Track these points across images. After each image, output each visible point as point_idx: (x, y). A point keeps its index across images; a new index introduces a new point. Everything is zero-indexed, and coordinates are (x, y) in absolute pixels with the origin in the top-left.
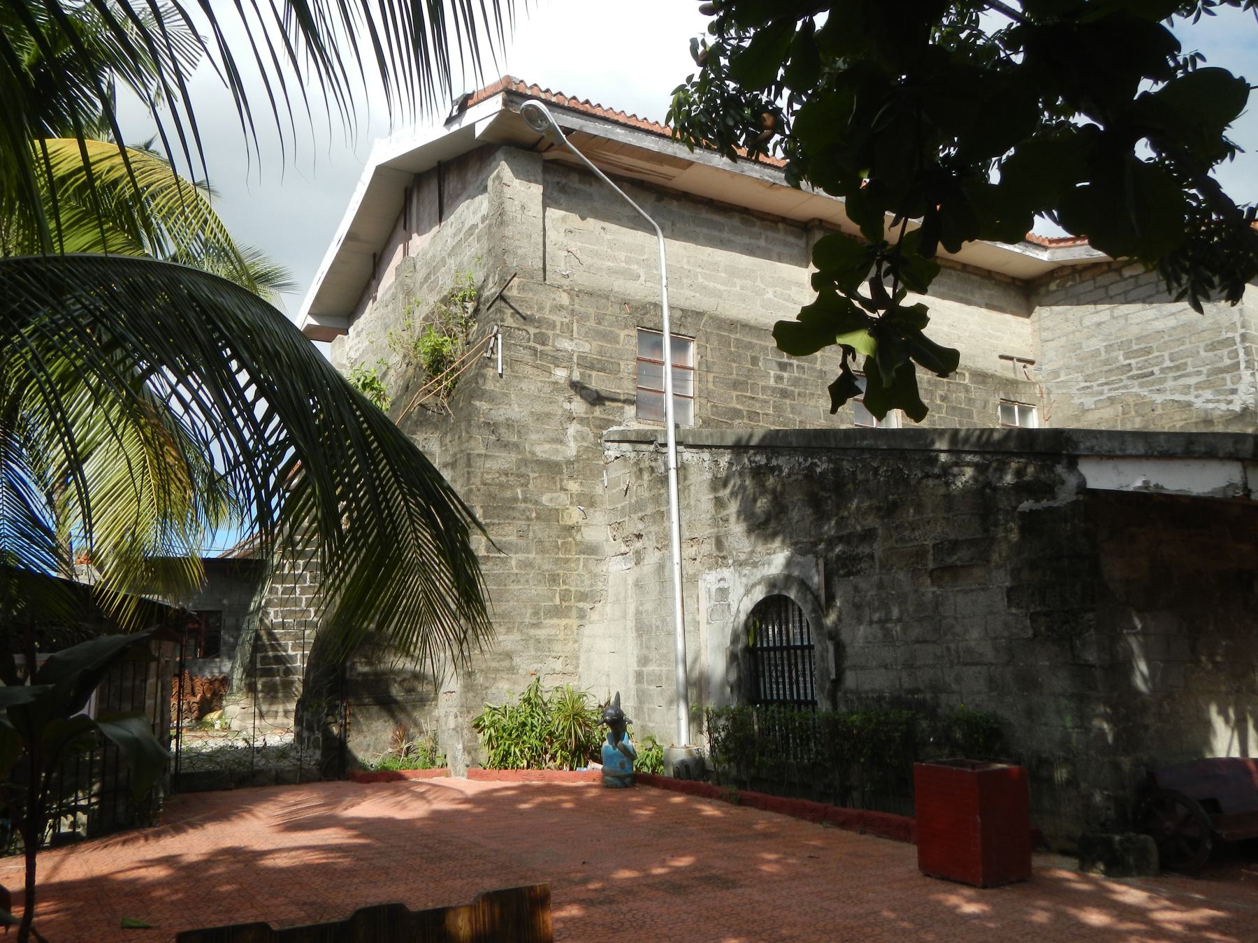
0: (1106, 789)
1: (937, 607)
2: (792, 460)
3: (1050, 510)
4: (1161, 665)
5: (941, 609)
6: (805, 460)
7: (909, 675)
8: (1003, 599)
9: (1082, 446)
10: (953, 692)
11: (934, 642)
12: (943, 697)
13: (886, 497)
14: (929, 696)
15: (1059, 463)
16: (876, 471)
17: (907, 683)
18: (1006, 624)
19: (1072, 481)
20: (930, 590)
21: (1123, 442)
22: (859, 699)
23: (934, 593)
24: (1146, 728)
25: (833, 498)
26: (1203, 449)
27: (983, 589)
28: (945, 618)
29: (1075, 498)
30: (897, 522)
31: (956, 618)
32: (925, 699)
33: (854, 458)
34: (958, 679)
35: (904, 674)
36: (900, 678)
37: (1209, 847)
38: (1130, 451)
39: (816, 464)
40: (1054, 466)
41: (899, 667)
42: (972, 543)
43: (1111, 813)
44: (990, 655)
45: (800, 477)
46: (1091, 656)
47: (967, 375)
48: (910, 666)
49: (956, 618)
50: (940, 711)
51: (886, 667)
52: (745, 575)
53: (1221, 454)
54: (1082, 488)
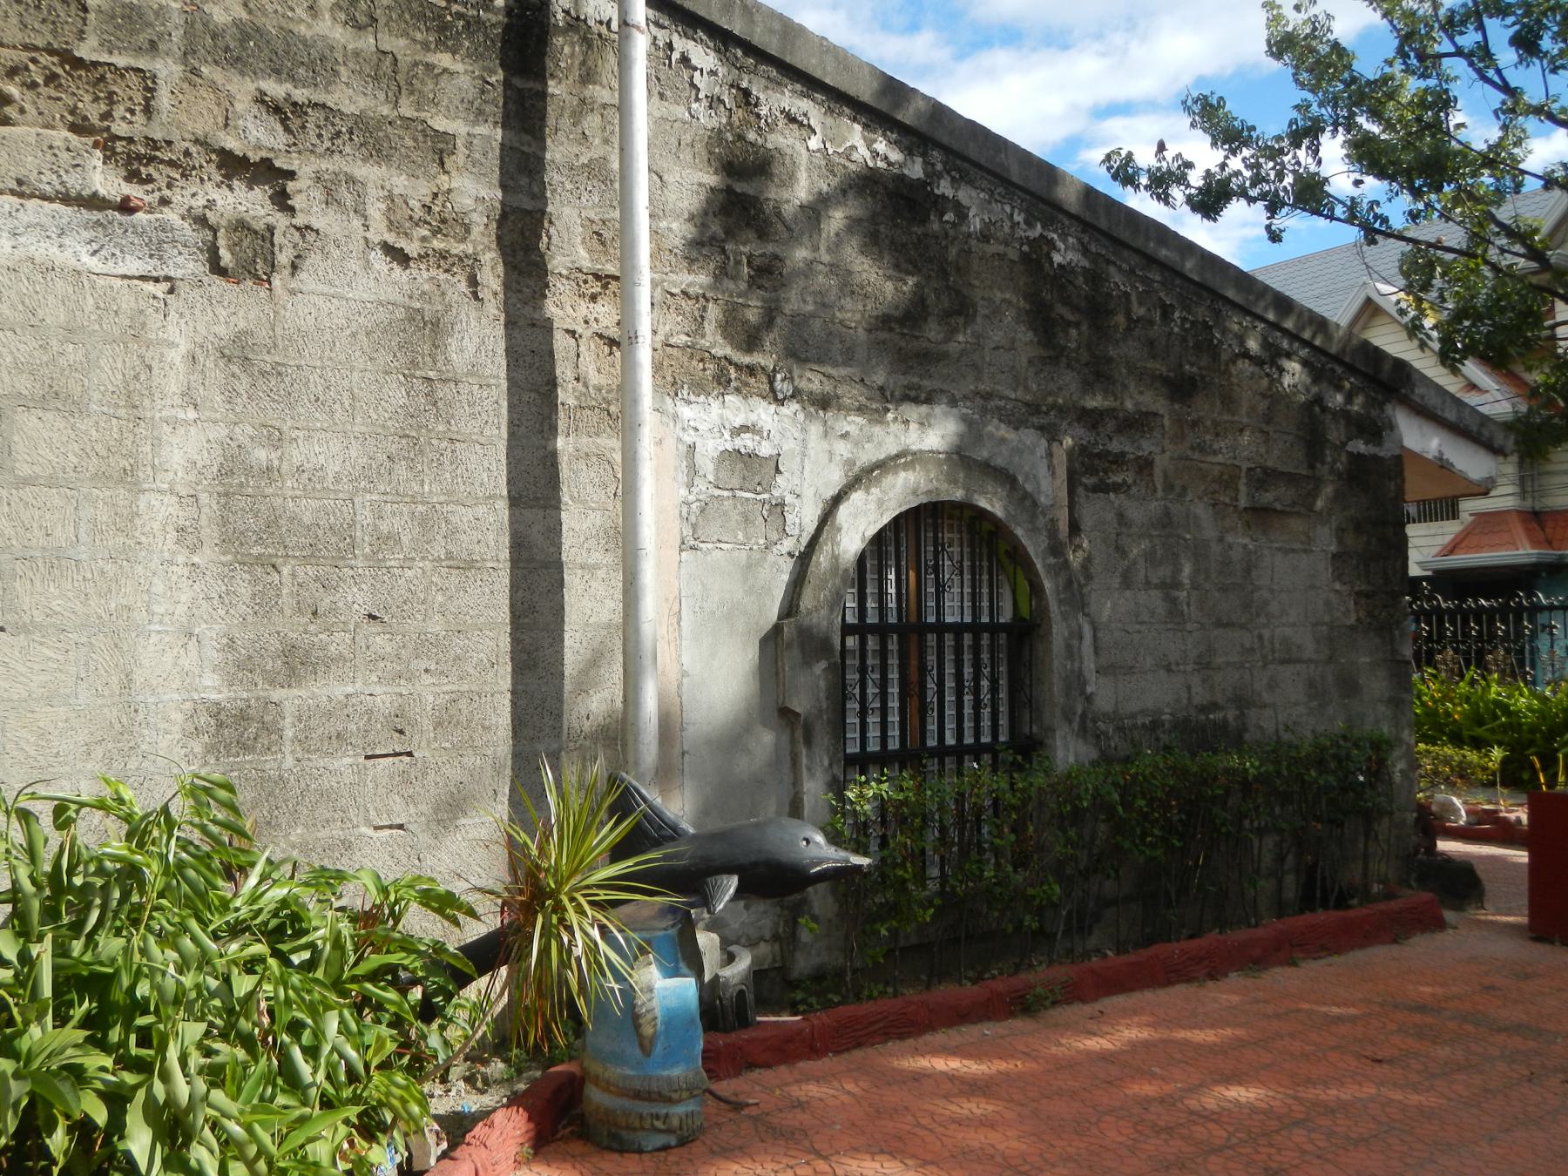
1: (1248, 570)
2: (996, 207)
3: (1375, 459)
5: (1254, 573)
6: (1029, 224)
7: (1204, 681)
8: (1327, 569)
10: (1265, 706)
11: (1242, 627)
12: (1252, 714)
13: (1181, 366)
14: (1231, 714)
16: (1166, 312)
17: (1200, 695)
18: (1328, 603)
20: (1241, 540)
22: (1120, 729)
23: (1245, 546)
25: (1084, 328)
27: (1305, 551)
28: (1259, 588)
30: (1194, 416)
31: (1272, 591)
32: (1225, 720)
33: (1132, 271)
34: (1272, 685)
35: (1195, 681)
36: (1189, 688)
39: (1051, 245)
41: (1189, 668)
42: (1291, 479)
44: (1309, 649)
45: (1013, 255)
48: (1204, 665)
49: (1272, 591)
50: (1247, 736)
51: (1169, 670)
52: (845, 436)
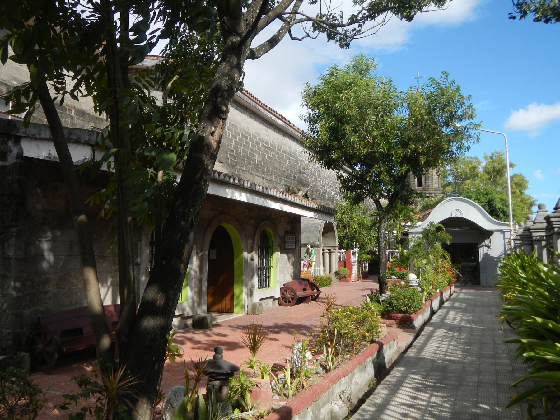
0: (9, 329)
4: (64, 258)
9: (21, 131)
15: (10, 140)
19: (15, 151)
21: (40, 131)
24: (47, 292)
26: (75, 138)
29: (15, 161)
37: (56, 357)
38: (43, 136)
40: (8, 141)
43: (10, 342)
46: (11, 253)
47: (73, 111)
53: (82, 141)
54: (20, 156)
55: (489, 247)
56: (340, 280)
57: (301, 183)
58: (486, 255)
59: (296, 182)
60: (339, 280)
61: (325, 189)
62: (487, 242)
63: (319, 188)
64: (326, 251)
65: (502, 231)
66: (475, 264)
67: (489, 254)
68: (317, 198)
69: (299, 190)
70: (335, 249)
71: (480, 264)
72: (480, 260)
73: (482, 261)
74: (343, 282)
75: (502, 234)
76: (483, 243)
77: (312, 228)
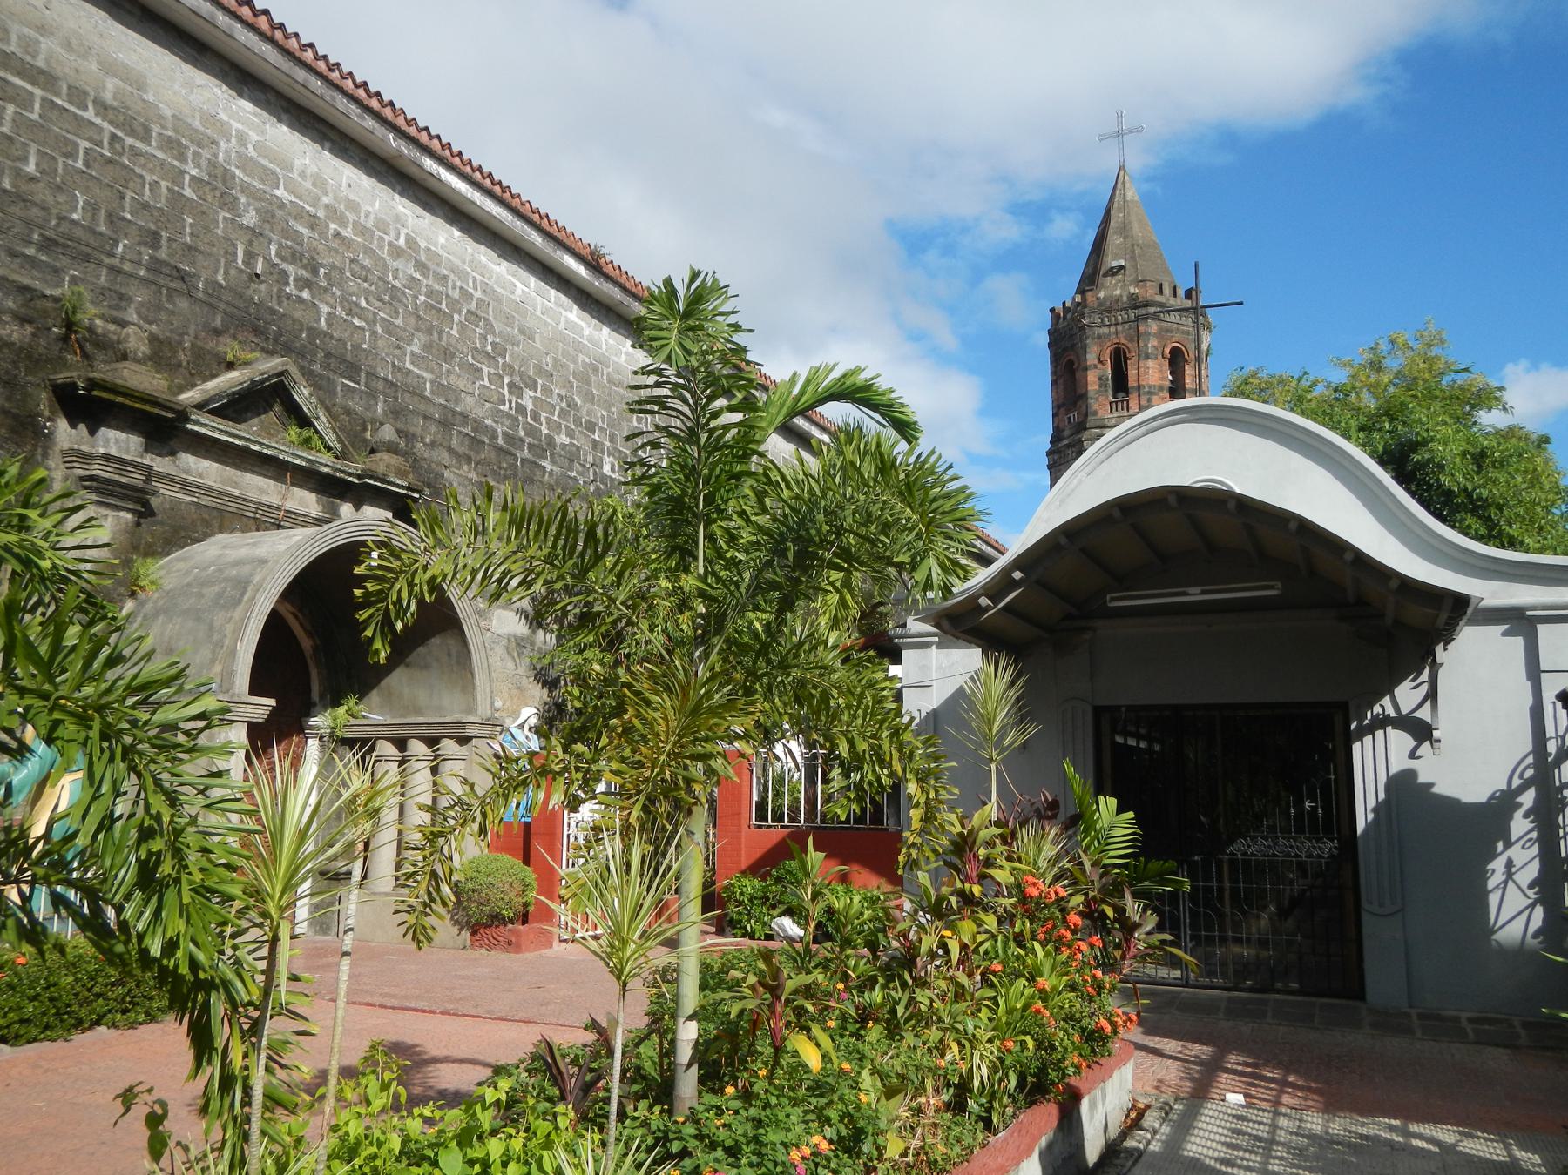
55: (1422, 732)
56: (473, 933)
57: (257, 331)
58: (1403, 787)
59: (183, 304)
60: (466, 934)
61: (532, 431)
62: (1407, 695)
63: (467, 404)
64: (417, 748)
65: (1519, 621)
66: (1329, 847)
67: (1422, 779)
68: (445, 457)
69: (230, 366)
70: (463, 740)
71: (1367, 858)
72: (1361, 826)
73: (1366, 831)
74: (489, 948)
75: (1519, 642)
76: (1385, 706)
77: (216, 588)
